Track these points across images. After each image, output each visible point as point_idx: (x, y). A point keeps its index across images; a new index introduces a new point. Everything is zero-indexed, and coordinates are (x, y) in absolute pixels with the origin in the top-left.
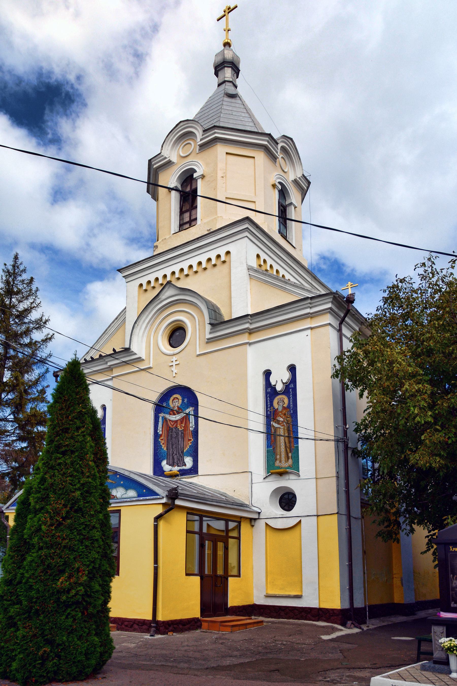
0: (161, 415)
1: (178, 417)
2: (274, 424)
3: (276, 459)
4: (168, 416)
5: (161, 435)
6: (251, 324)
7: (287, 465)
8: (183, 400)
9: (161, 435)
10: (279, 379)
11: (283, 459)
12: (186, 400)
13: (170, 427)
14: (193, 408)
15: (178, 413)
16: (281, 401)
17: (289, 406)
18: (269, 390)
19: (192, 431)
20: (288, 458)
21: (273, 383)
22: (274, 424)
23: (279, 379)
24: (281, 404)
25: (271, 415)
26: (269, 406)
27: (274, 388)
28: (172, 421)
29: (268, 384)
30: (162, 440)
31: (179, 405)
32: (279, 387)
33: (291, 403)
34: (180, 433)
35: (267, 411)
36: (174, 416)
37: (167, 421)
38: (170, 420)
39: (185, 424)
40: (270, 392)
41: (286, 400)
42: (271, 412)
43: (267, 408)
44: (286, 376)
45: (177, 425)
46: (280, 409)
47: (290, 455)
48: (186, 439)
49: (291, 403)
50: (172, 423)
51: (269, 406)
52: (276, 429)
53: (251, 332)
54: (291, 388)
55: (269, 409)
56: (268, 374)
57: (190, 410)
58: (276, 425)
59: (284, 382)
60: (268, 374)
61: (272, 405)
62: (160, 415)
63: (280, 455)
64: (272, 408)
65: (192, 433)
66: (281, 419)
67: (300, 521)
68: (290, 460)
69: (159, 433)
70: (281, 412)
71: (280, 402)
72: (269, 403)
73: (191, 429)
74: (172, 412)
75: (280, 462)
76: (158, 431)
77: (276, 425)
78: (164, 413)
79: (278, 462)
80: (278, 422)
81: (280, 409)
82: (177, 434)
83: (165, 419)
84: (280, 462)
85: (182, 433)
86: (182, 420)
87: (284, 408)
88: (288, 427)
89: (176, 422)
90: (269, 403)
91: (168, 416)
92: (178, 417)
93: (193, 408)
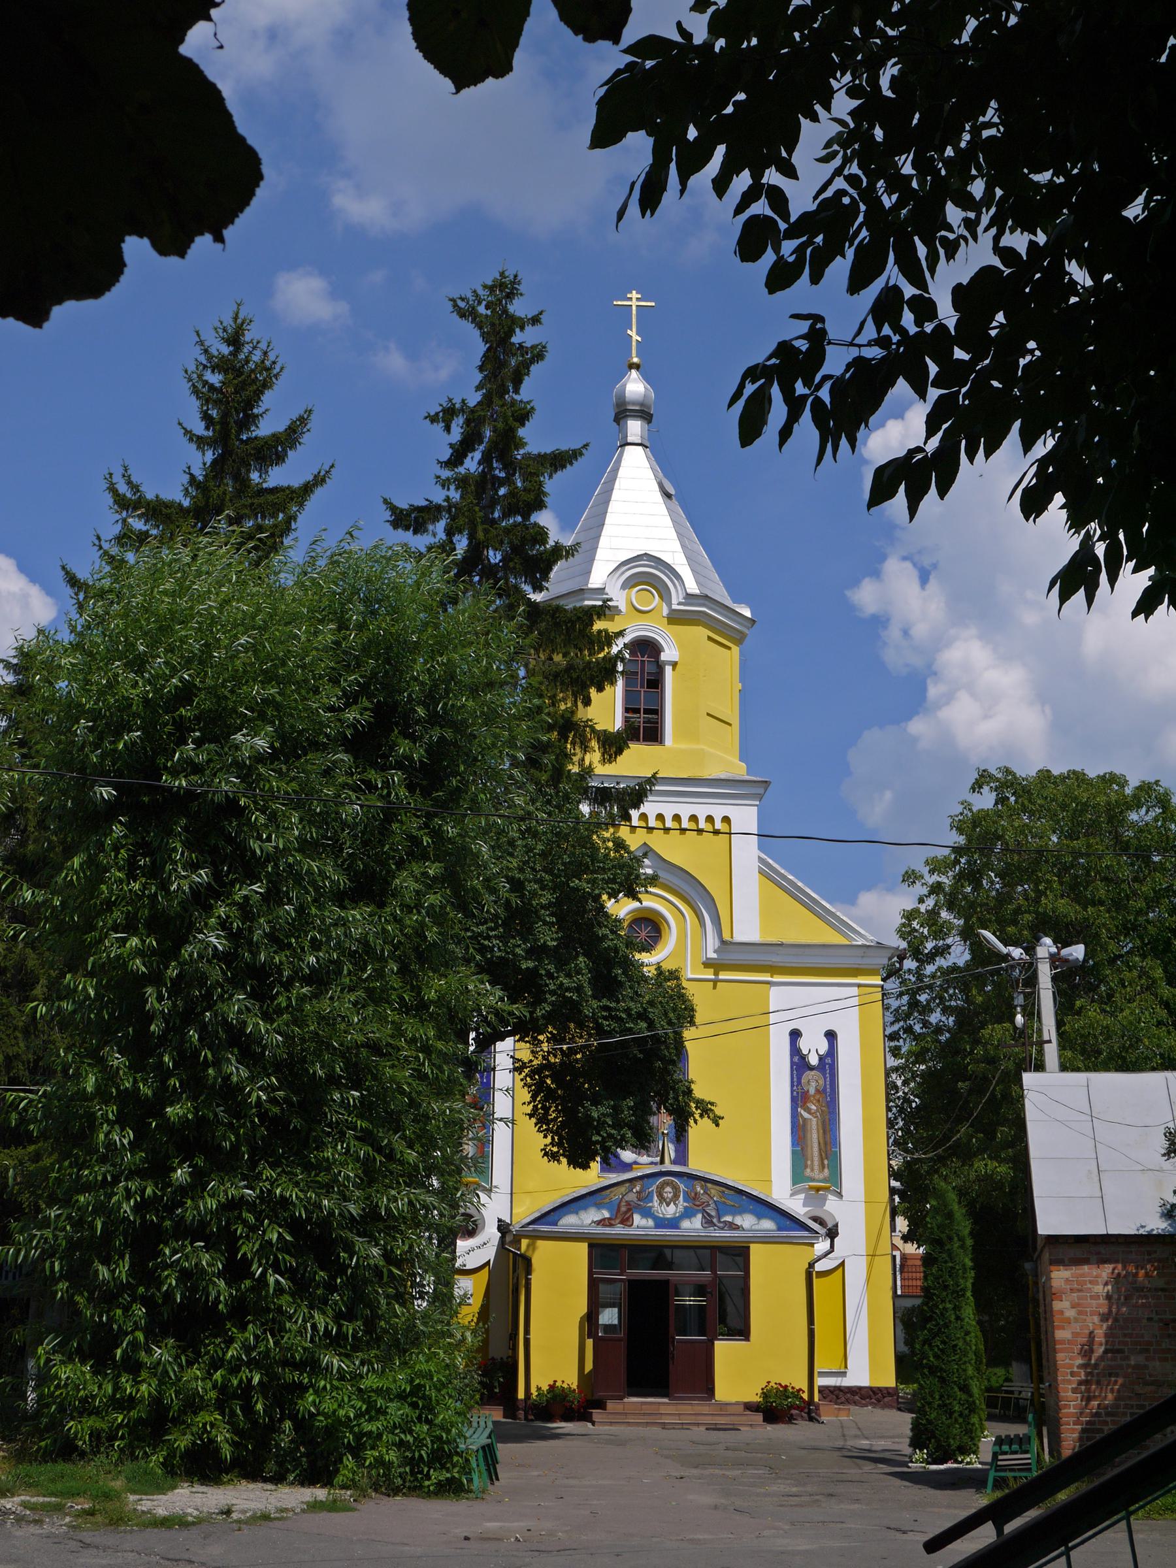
3: (806, 1167)
7: (821, 1176)
10: (813, 1046)
11: (816, 1167)
16: (814, 1081)
17: (825, 1090)
18: (796, 1059)
20: (823, 1168)
21: (805, 1052)
23: (813, 1046)
24: (813, 1084)
25: (798, 1099)
27: (803, 1058)
29: (795, 1051)
32: (814, 1060)
35: (792, 1092)
40: (799, 1063)
41: (821, 1082)
43: (792, 1086)
44: (823, 1047)
46: (812, 1091)
47: (826, 1162)
52: (805, 1120)
54: (829, 1063)
56: (795, 1035)
58: (806, 1115)
59: (821, 1053)
60: (795, 1035)
61: (799, 1083)
63: (812, 1161)
66: (813, 1107)
67: (843, 1262)
68: (826, 1170)
71: (813, 1082)
75: (812, 1170)
77: (806, 1115)
79: (808, 1170)
80: (809, 1111)
81: (812, 1091)
84: (812, 1170)
87: (817, 1091)
88: (824, 1122)
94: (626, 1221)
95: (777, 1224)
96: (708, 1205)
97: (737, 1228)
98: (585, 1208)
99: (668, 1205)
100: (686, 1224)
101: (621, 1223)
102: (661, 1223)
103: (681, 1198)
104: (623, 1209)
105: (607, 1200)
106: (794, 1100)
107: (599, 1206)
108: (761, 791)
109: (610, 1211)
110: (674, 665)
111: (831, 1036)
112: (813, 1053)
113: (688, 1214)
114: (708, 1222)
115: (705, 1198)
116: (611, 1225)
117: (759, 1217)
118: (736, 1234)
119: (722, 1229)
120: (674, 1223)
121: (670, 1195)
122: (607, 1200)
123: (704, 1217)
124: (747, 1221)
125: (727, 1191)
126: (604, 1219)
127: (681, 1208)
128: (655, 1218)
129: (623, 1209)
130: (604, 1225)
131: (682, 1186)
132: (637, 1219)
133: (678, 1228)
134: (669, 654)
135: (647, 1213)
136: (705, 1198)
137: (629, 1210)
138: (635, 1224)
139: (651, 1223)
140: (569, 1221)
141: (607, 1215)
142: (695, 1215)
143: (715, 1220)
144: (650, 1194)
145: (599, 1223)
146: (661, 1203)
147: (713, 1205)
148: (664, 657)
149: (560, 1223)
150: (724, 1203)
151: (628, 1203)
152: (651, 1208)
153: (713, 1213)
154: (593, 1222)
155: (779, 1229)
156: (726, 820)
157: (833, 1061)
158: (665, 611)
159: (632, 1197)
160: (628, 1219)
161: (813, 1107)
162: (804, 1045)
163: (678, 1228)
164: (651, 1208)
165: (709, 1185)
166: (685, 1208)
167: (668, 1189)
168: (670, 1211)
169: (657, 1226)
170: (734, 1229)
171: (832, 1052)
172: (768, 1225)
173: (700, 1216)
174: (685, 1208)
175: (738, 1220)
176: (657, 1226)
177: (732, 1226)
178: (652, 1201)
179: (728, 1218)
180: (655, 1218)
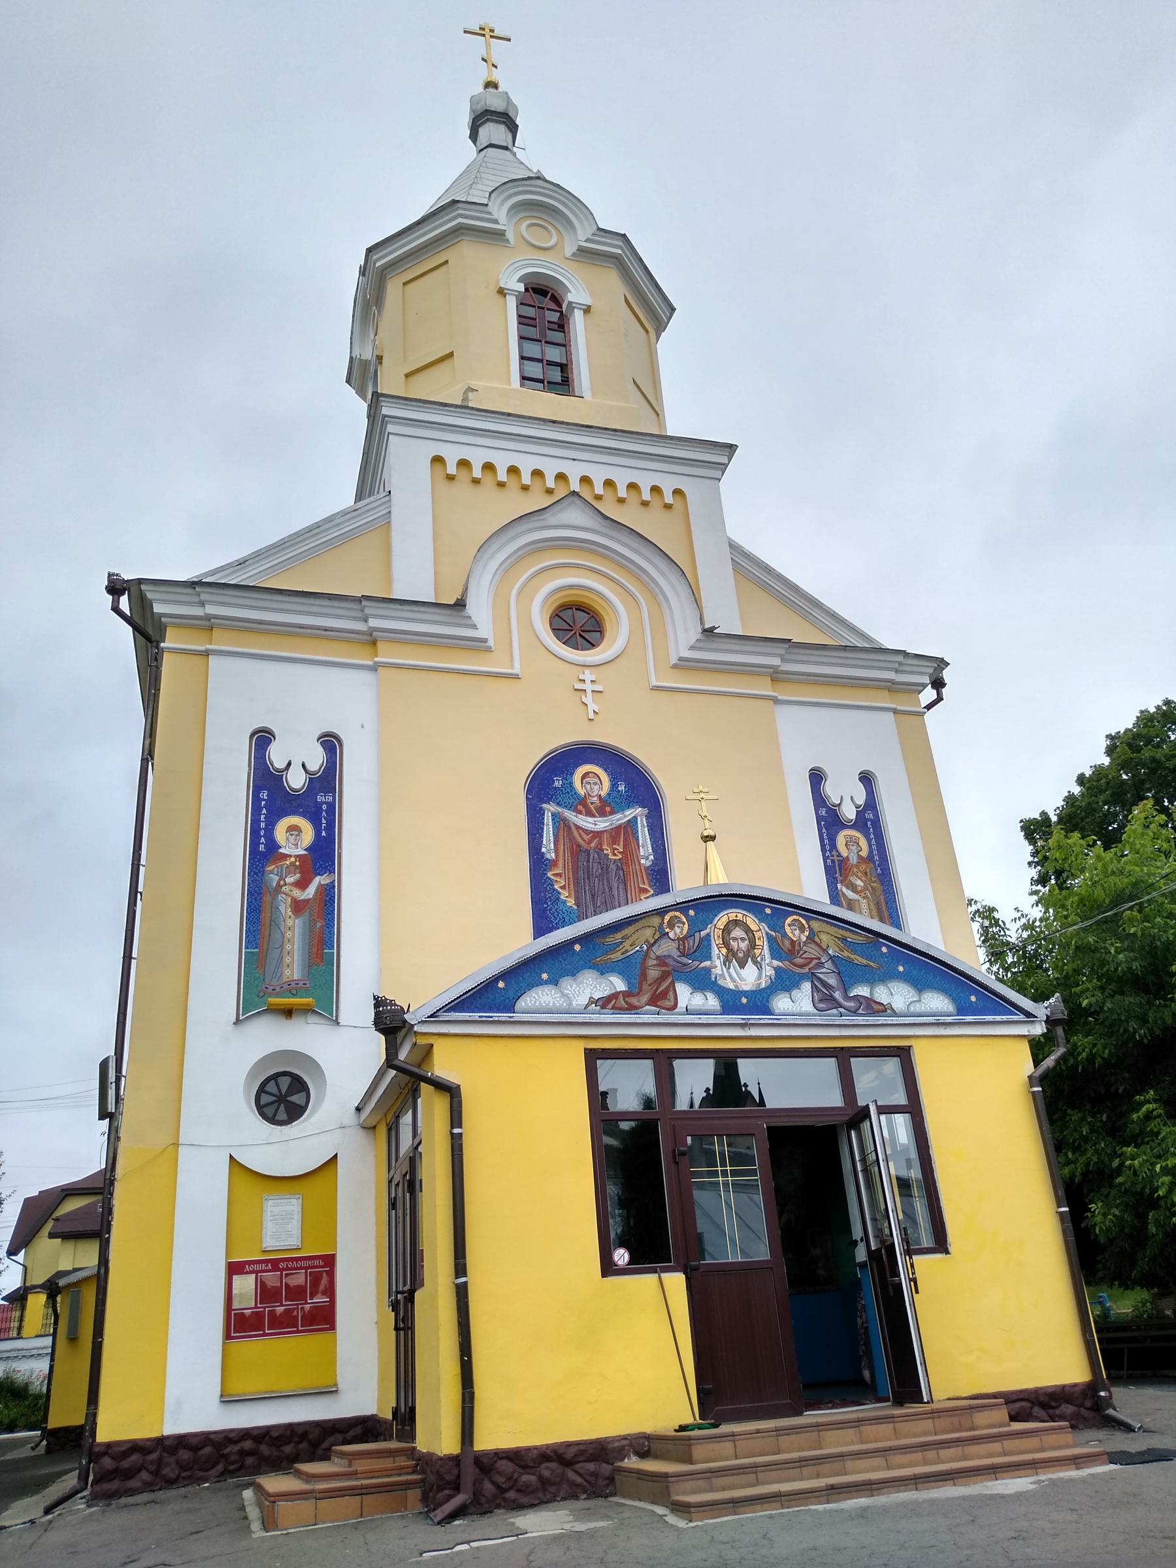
0: (550, 808)
1: (601, 824)
2: (844, 890)
4: (569, 815)
5: (554, 863)
6: (783, 660)
8: (614, 786)
9: (554, 863)
10: (846, 795)
12: (622, 788)
13: (579, 846)
14: (646, 811)
15: (602, 813)
17: (870, 858)
18: (823, 812)
19: (646, 868)
22: (844, 890)
26: (828, 848)
28: (587, 832)
30: (559, 875)
31: (603, 793)
33: (875, 852)
34: (612, 867)
36: (591, 820)
37: (569, 828)
38: (578, 828)
39: (624, 847)
40: (829, 821)
41: (863, 843)
42: (833, 861)
43: (823, 850)
45: (601, 844)
46: (854, 860)
48: (631, 885)
49: (875, 852)
50: (586, 837)
51: (828, 848)
53: (776, 676)
54: (869, 820)
55: (828, 854)
56: (817, 778)
57: (637, 812)
58: (850, 894)
60: (817, 778)
61: (833, 846)
62: (544, 805)
64: (834, 853)
65: (648, 875)
69: (548, 856)
70: (857, 866)
72: (826, 841)
73: (643, 861)
74: (581, 805)
76: (543, 850)
78: (558, 804)
80: (853, 888)
81: (854, 860)
82: (605, 869)
83: (561, 823)
85: (618, 868)
86: (615, 833)
87: (860, 857)
88: (878, 904)
89: (598, 834)
90: (826, 841)
91: (569, 815)
92: (601, 824)
93: (646, 811)
94: (662, 998)
95: (954, 1000)
96: (820, 965)
97: (884, 1009)
98: (573, 973)
99: (742, 965)
100: (782, 1003)
101: (653, 1001)
102: (731, 1002)
103: (766, 952)
104: (653, 973)
105: (618, 956)
106: (830, 871)
107: (603, 970)
108: (724, 460)
109: (627, 979)
110: (587, 310)
111: (866, 779)
112: (847, 800)
113: (784, 982)
114: (825, 999)
115: (812, 951)
116: (631, 1008)
117: (920, 986)
118: (882, 1020)
119: (855, 1012)
120: (757, 1003)
121: (744, 945)
122: (618, 956)
123: (814, 988)
124: (897, 995)
125: (851, 937)
126: (615, 996)
127: (769, 972)
128: (721, 992)
129: (653, 973)
130: (617, 1009)
131: (764, 926)
132: (683, 991)
133: (768, 1011)
134: (576, 294)
135: (703, 982)
136: (812, 951)
137: (664, 976)
138: (682, 1004)
139: (712, 1001)
140: (540, 998)
141: (620, 985)
142: (797, 985)
143: (837, 995)
144: (706, 941)
145: (605, 1003)
146: (727, 961)
147: (829, 965)
148: (570, 297)
149: (521, 1004)
150: (850, 962)
151: (662, 961)
152: (708, 970)
153: (832, 981)
154: (592, 1001)
155: (961, 1011)
156: (677, 492)
157: (877, 816)
158: (569, 249)
159: (666, 948)
160: (664, 995)
161: (859, 883)
162: (832, 791)
163: (768, 1011)
164: (708, 970)
165: (816, 925)
166: (777, 970)
167: (738, 933)
168: (748, 978)
169: (726, 1009)
170: (874, 1013)
171: (871, 803)
172: (937, 1002)
173: (807, 986)
174: (777, 969)
175: (881, 994)
176: (726, 1009)
177: (872, 1007)
178: (709, 957)
179: (862, 991)
180: (721, 992)
